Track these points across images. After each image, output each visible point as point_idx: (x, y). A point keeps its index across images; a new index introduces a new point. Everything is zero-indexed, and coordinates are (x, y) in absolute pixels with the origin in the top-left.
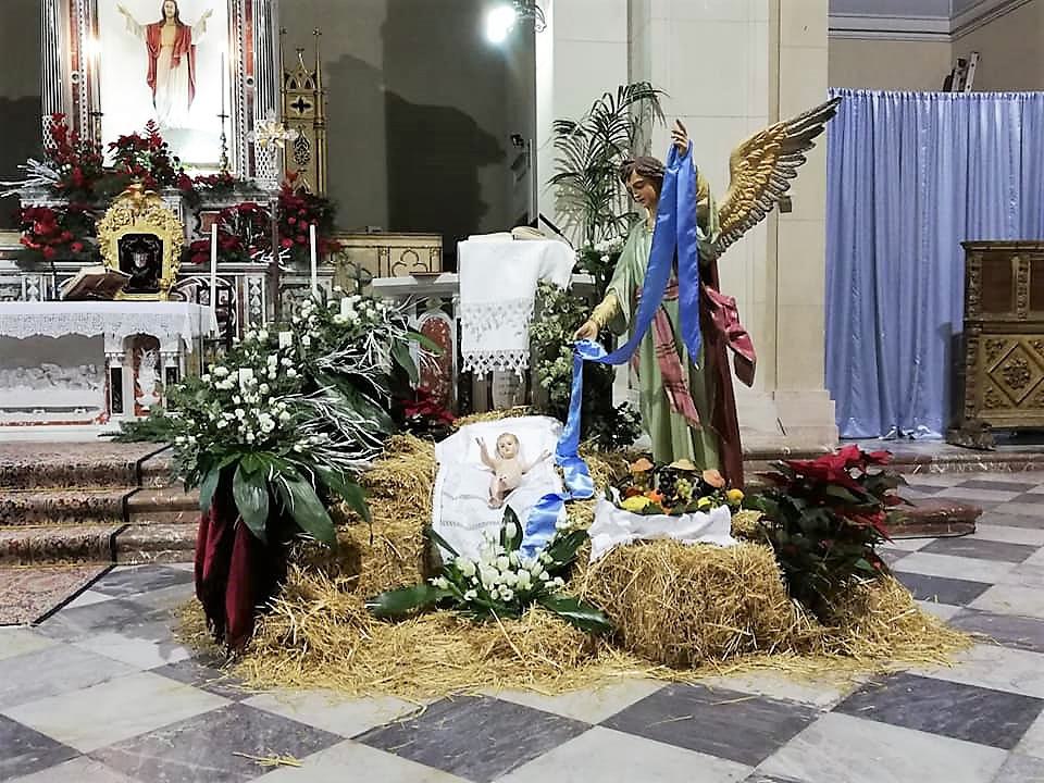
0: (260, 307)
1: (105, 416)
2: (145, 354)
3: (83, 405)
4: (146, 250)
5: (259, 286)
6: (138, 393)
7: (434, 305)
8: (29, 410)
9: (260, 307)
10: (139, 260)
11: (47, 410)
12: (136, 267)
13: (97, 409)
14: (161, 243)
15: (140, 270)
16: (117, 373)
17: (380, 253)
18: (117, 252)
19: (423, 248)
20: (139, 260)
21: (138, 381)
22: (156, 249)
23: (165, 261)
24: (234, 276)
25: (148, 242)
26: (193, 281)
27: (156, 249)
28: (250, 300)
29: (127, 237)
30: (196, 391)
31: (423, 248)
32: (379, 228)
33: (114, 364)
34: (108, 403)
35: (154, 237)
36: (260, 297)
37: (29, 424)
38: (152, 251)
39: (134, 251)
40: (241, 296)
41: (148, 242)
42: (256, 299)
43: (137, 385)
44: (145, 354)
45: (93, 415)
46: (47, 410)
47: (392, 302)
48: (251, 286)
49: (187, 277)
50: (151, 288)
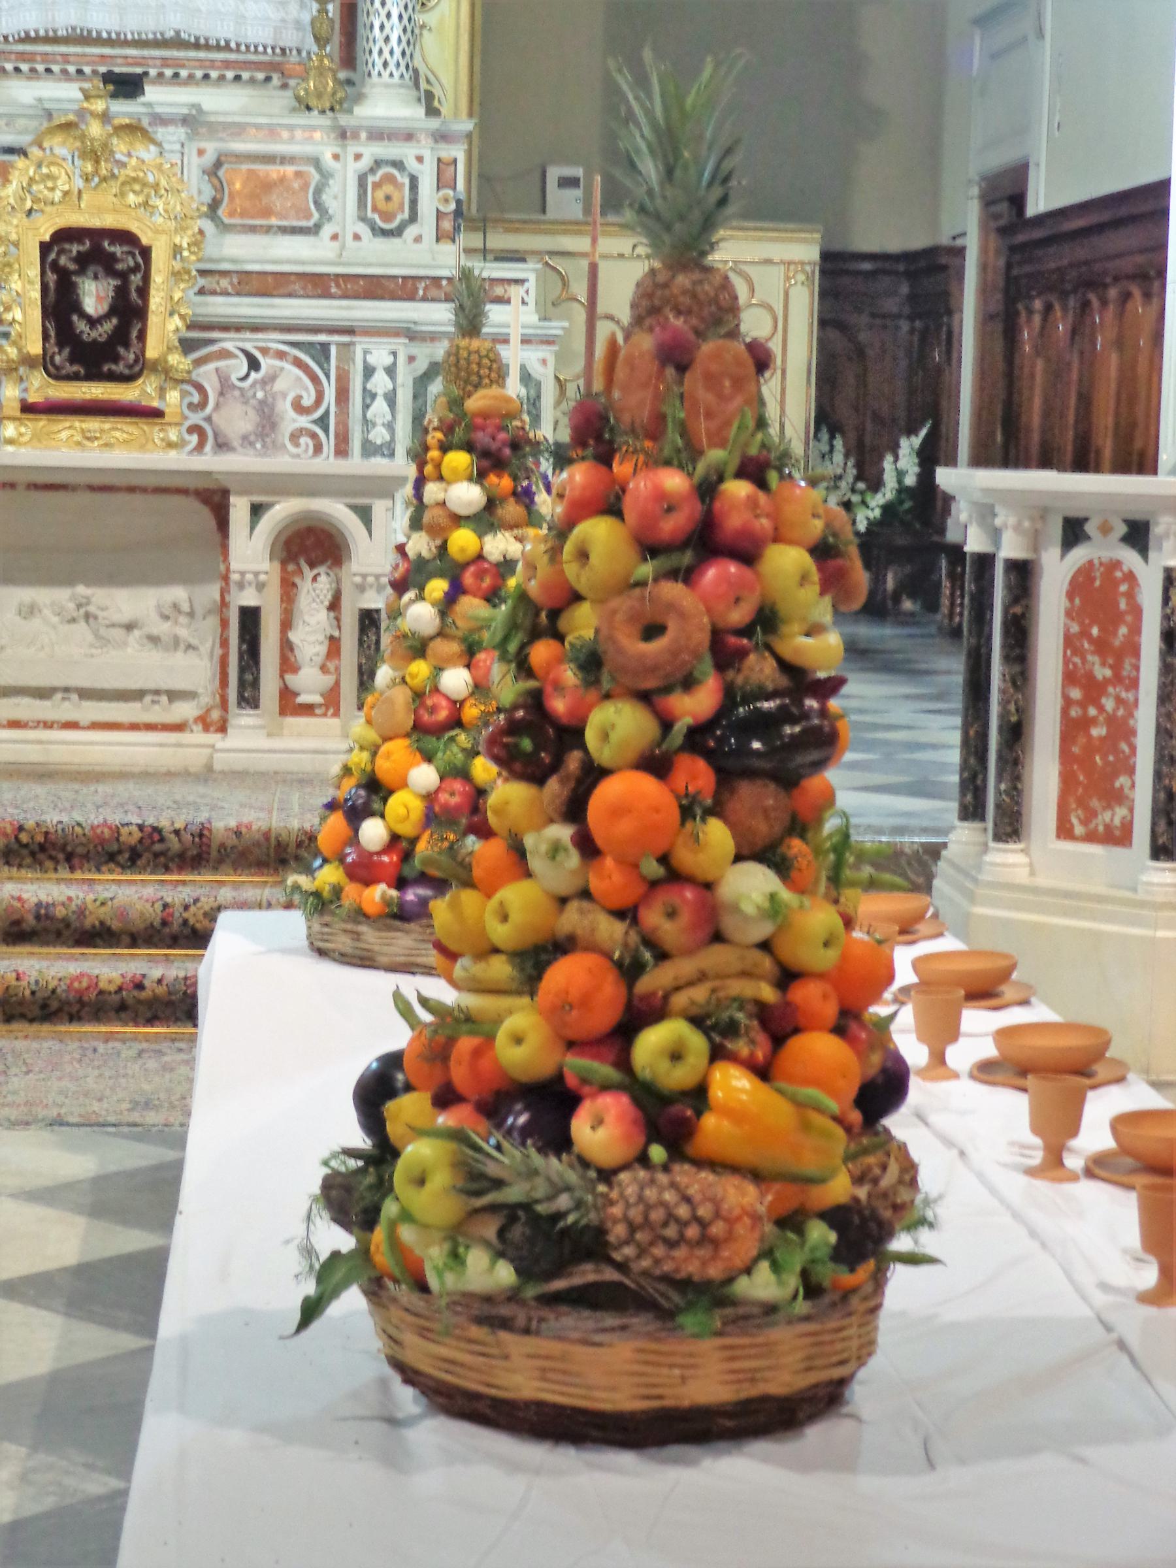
0: (390, 427)
1: (215, 715)
2: (309, 574)
3: (164, 686)
4: (111, 272)
5: (391, 371)
6: (288, 664)
7: (1105, 529)
9: (390, 427)
11: (86, 694)
12: (83, 315)
14: (146, 252)
15: (93, 322)
16: (250, 618)
18: (34, 272)
19: (768, 262)
21: (293, 636)
22: (135, 269)
23: (156, 301)
24: (325, 347)
25: (118, 250)
26: (225, 354)
27: (135, 269)
28: (366, 407)
29: (64, 236)
30: (524, 668)
31: (768, 262)
32: (579, 172)
33: (249, 598)
34: (224, 682)
35: (126, 237)
36: (391, 399)
37: (48, 725)
38: (123, 276)
39: (82, 271)
40: (343, 395)
41: (118, 250)
42: (380, 407)
43: (287, 646)
44: (309, 574)
45: (185, 710)
46: (86, 694)
47: (1012, 521)
49: (211, 342)
50: (120, 368)
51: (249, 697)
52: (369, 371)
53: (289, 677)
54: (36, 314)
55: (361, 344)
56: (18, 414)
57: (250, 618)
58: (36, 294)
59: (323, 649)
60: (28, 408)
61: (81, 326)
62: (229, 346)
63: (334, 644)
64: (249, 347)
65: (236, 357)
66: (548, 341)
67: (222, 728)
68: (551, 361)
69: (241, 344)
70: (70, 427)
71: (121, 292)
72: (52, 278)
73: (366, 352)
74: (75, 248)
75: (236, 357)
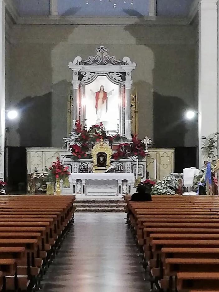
8: (103, 193)
10: (101, 159)
13: (115, 193)
15: (102, 161)
16: (120, 186)
17: (157, 153)
20: (101, 159)
21: (123, 188)
23: (107, 159)
24: (123, 163)
29: (99, 153)
33: (120, 185)
42: (129, 168)
43: (123, 189)
45: (115, 194)
48: (127, 165)
52: (127, 165)
57: (120, 186)
58: (96, 159)
59: (126, 189)
60: (96, 170)
61: (100, 162)
63: (127, 188)
67: (118, 195)
71: (104, 158)
72: (98, 157)
74: (100, 154)
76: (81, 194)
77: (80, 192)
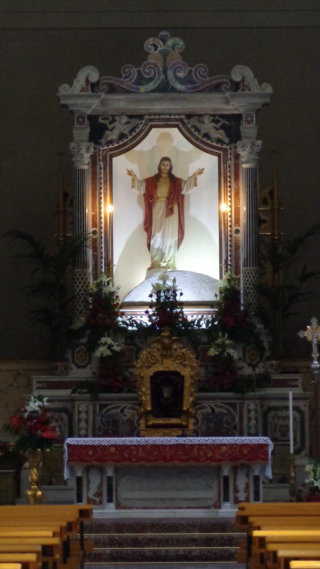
6: (236, 491)
26: (204, 407)
28: (249, 422)
51: (226, 499)
52: (249, 411)
53: (236, 494)
54: (149, 397)
55: (247, 402)
56: (144, 428)
62: (205, 405)
64: (212, 405)
65: (208, 408)
66: (305, 399)
68: (307, 404)
69: (208, 404)
70: (160, 432)
73: (248, 405)
75: (208, 408)
76: (101, 503)
77: (98, 499)
